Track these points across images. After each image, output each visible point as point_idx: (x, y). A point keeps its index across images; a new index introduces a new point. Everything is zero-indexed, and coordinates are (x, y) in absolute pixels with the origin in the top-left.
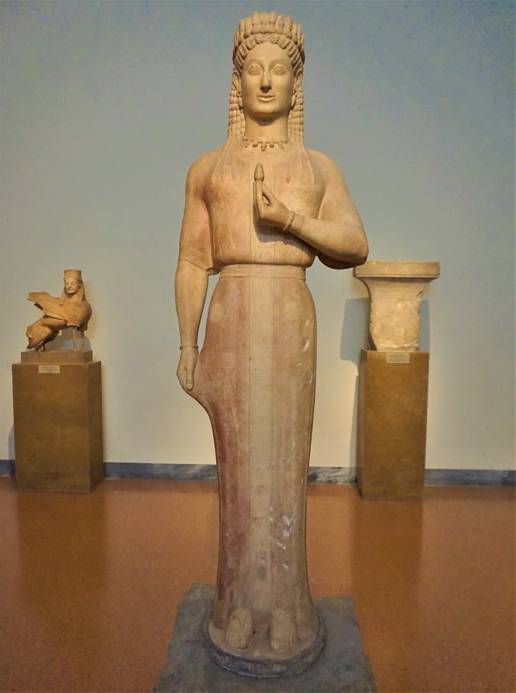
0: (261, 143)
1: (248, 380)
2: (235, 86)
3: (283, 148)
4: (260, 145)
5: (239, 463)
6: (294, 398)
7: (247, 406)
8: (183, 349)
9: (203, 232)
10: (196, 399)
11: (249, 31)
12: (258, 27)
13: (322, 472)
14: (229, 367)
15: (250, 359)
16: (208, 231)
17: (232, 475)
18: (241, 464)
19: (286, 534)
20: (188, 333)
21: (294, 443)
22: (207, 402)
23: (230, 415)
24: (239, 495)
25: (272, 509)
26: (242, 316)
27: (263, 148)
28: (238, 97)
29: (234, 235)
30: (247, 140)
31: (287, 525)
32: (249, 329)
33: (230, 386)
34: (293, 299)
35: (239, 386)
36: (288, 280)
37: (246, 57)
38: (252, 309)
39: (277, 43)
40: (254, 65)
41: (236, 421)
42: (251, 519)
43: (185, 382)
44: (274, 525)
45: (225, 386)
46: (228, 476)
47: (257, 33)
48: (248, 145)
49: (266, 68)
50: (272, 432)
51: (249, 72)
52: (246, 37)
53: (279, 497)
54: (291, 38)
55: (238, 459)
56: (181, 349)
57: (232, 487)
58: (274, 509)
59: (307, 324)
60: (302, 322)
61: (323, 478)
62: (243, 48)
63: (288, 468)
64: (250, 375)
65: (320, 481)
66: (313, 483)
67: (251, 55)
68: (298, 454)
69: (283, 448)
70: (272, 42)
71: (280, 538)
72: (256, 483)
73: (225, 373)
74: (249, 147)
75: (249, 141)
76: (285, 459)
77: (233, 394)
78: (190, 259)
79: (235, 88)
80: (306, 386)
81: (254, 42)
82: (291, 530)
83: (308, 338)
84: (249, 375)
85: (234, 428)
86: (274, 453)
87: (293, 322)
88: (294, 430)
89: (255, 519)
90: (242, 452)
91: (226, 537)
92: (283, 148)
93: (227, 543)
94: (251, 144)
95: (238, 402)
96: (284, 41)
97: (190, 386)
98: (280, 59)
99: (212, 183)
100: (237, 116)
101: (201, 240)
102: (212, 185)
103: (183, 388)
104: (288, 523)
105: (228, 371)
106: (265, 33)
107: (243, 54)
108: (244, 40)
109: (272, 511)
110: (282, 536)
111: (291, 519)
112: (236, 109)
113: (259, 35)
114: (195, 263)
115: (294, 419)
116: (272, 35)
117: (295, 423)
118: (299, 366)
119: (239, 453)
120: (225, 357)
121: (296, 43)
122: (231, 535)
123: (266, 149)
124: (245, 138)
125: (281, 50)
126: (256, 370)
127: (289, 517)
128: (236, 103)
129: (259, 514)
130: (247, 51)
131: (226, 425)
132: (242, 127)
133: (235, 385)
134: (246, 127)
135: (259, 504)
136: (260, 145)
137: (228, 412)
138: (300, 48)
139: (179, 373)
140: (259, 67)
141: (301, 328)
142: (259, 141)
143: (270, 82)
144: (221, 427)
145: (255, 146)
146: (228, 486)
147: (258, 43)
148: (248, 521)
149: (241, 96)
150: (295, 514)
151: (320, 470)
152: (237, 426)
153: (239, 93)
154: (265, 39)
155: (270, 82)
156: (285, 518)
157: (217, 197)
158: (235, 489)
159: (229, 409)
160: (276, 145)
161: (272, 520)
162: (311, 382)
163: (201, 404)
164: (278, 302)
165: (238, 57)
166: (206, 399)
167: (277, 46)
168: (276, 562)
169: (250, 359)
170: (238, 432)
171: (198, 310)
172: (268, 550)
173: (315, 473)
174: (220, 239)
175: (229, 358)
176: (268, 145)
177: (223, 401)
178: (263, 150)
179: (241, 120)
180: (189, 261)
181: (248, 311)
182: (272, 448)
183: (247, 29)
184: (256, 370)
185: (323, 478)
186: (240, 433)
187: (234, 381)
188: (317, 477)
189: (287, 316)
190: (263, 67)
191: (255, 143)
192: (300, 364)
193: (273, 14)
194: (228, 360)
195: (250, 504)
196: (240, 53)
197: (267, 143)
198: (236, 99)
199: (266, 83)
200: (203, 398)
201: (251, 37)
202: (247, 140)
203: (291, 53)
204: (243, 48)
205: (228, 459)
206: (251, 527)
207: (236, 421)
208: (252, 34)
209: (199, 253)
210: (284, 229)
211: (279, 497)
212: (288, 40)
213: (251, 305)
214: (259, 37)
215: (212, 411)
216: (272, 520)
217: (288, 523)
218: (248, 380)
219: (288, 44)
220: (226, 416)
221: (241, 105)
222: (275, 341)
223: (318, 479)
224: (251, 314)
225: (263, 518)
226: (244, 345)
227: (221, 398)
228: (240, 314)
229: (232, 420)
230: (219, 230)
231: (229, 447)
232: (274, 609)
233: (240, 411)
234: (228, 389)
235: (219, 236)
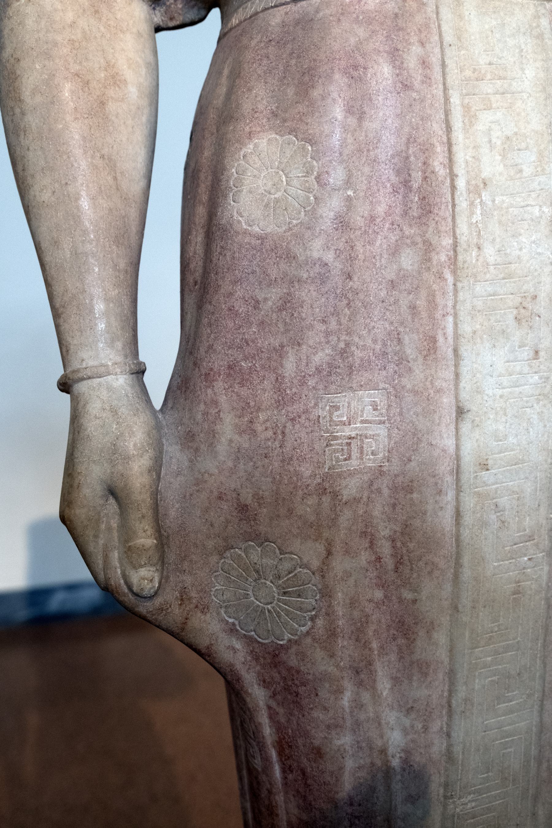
1: (446, 519)
7: (441, 638)
8: (81, 388)
14: (354, 463)
15: (460, 412)
20: (100, 307)
22: (238, 645)
23: (366, 697)
26: (421, 194)
32: (454, 260)
33: (365, 557)
38: (461, 156)
41: (391, 717)
43: (115, 555)
45: (340, 564)
56: (65, 386)
73: (335, 495)
77: (379, 594)
84: (450, 495)
120: (341, 416)
126: (485, 467)
131: (345, 740)
133: (385, 549)
137: (360, 684)
139: (80, 513)
159: (362, 672)
166: (232, 630)
169: (460, 412)
171: (137, 187)
181: (442, 172)
184: (485, 467)
187: (384, 531)
194: (348, 431)
207: (391, 717)
213: (458, 135)
218: (446, 519)
224: (461, 183)
227: (320, 622)
228: (406, 183)
233: (413, 667)
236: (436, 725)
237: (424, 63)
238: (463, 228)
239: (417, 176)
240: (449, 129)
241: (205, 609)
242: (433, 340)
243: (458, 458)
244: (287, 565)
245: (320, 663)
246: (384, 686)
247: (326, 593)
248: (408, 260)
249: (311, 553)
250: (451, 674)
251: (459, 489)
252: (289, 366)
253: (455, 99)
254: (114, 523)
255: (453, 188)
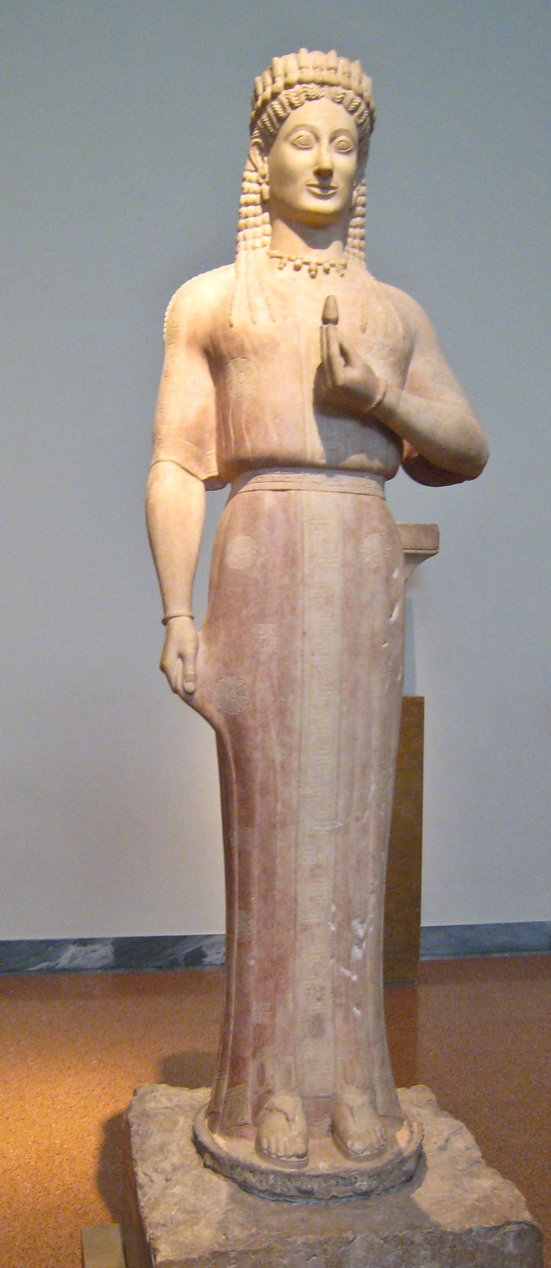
0: (307, 263)
2: (254, 165)
3: (342, 276)
4: (305, 268)
5: (278, 826)
6: (376, 704)
9: (204, 411)
10: (200, 711)
11: (293, 77)
12: (309, 74)
13: (213, 945)
16: (212, 410)
17: (267, 850)
18: (284, 825)
19: (357, 953)
21: (373, 787)
22: (222, 717)
24: (279, 884)
25: (333, 908)
26: (292, 559)
27: (313, 273)
28: (260, 184)
29: (275, 417)
30: (281, 258)
31: (358, 937)
34: (374, 530)
35: (284, 685)
36: (365, 498)
37: (286, 118)
39: (340, 103)
40: (302, 132)
42: (298, 928)
44: (338, 937)
45: (259, 685)
46: (256, 853)
47: (308, 83)
48: (285, 265)
49: (325, 141)
50: (339, 766)
51: (294, 145)
52: (288, 86)
53: (346, 885)
54: (361, 96)
55: (278, 818)
57: (264, 870)
58: (338, 906)
59: (396, 575)
60: (390, 571)
61: (215, 957)
62: (282, 104)
63: (364, 831)
64: (303, 661)
65: (211, 965)
66: (198, 968)
67: (295, 118)
68: (379, 806)
69: (356, 794)
70: (333, 100)
71: (345, 960)
72: (308, 859)
74: (285, 269)
75: (285, 260)
76: (359, 814)
78: (178, 460)
79: (253, 169)
80: (393, 685)
81: (303, 97)
82: (364, 945)
83: (396, 601)
85: (273, 761)
86: (341, 803)
87: (376, 571)
88: (374, 762)
89: (306, 928)
90: (284, 805)
91: (249, 966)
92: (342, 276)
93: (252, 976)
94: (290, 265)
95: (282, 712)
96: (352, 101)
97: (190, 686)
98: (346, 128)
99: (231, 326)
100: (255, 216)
101: (199, 426)
102: (234, 329)
103: (176, 691)
104: (361, 933)
105: (263, 658)
106: (322, 84)
107: (281, 113)
108: (284, 92)
109: (334, 912)
110: (349, 955)
111: (365, 925)
112: (254, 204)
113: (312, 85)
114: (187, 466)
115: (375, 743)
116: (334, 88)
117: (376, 751)
118: (385, 648)
119: (279, 807)
121: (368, 105)
122: (259, 961)
123: (318, 276)
124: (275, 252)
125: (345, 115)
127: (362, 922)
128: (255, 193)
129: (313, 918)
130: (289, 110)
131: (258, 755)
132: (265, 235)
133: (275, 681)
134: (273, 235)
135: (312, 899)
136: (305, 268)
138: (371, 113)
140: (312, 137)
141: (388, 580)
142: (305, 260)
143: (332, 164)
144: (248, 760)
145: (297, 269)
146: (256, 872)
147: (309, 99)
148: (292, 933)
149: (268, 184)
150: (371, 916)
151: (213, 940)
152: (278, 758)
153: (264, 177)
154: (322, 94)
155: (332, 164)
156: (355, 923)
157: (242, 351)
158: (269, 873)
159: (265, 726)
160: (332, 270)
161: (333, 928)
162: (400, 677)
163: (209, 720)
164: (352, 533)
165: (269, 116)
166: (219, 711)
167: (340, 107)
168: (340, 1005)
169: (304, 634)
170: (278, 768)
172: (328, 984)
173: (199, 949)
174: (247, 422)
175: (268, 632)
176: (320, 269)
177: (255, 710)
178: (313, 277)
179: (264, 223)
180: (177, 464)
182: (337, 795)
183: (289, 75)
184: (313, 655)
185: (215, 957)
186: (282, 767)
187: (275, 674)
188: (205, 956)
189: (367, 560)
190: (317, 138)
191: (298, 262)
192: (385, 645)
193: (333, 54)
194: (262, 638)
195: (296, 902)
196: (275, 111)
197: (319, 264)
198: (255, 187)
199: (326, 165)
200: (212, 709)
201: (298, 88)
202: (281, 258)
203: (361, 121)
204: (282, 104)
205: (258, 819)
206: (297, 944)
207: (276, 748)
208: (300, 82)
209: (195, 449)
210: (367, 410)
211: (346, 885)
212: (358, 100)
214: (313, 89)
215: (230, 732)
216: (333, 928)
217: (361, 933)
218: (298, 673)
219: (358, 107)
220: (259, 738)
221: (267, 197)
222: (347, 604)
223: (207, 960)
224: (306, 554)
225: (319, 925)
226: (293, 610)
229: (267, 748)
230: (245, 407)
231: (263, 796)
232: (342, 1088)
233: (285, 729)
234: (263, 691)
235: (244, 418)
236: (295, 755)
237: (295, 514)
238: (306, 570)
239: (290, 552)
240: (303, 536)
241: (210, 702)
242: (294, 608)
243: (303, 651)
244: (239, 684)
245: (250, 722)
246: (274, 734)
247: (253, 694)
248: (286, 580)
249: (249, 679)
250: (300, 735)
251: (303, 661)
252: (244, 613)
253: (305, 526)
254: (181, 666)
255: (303, 556)
